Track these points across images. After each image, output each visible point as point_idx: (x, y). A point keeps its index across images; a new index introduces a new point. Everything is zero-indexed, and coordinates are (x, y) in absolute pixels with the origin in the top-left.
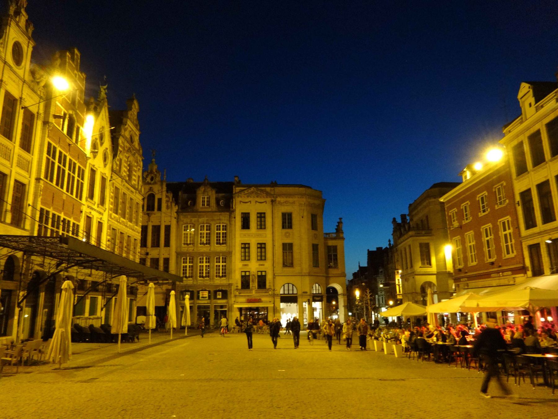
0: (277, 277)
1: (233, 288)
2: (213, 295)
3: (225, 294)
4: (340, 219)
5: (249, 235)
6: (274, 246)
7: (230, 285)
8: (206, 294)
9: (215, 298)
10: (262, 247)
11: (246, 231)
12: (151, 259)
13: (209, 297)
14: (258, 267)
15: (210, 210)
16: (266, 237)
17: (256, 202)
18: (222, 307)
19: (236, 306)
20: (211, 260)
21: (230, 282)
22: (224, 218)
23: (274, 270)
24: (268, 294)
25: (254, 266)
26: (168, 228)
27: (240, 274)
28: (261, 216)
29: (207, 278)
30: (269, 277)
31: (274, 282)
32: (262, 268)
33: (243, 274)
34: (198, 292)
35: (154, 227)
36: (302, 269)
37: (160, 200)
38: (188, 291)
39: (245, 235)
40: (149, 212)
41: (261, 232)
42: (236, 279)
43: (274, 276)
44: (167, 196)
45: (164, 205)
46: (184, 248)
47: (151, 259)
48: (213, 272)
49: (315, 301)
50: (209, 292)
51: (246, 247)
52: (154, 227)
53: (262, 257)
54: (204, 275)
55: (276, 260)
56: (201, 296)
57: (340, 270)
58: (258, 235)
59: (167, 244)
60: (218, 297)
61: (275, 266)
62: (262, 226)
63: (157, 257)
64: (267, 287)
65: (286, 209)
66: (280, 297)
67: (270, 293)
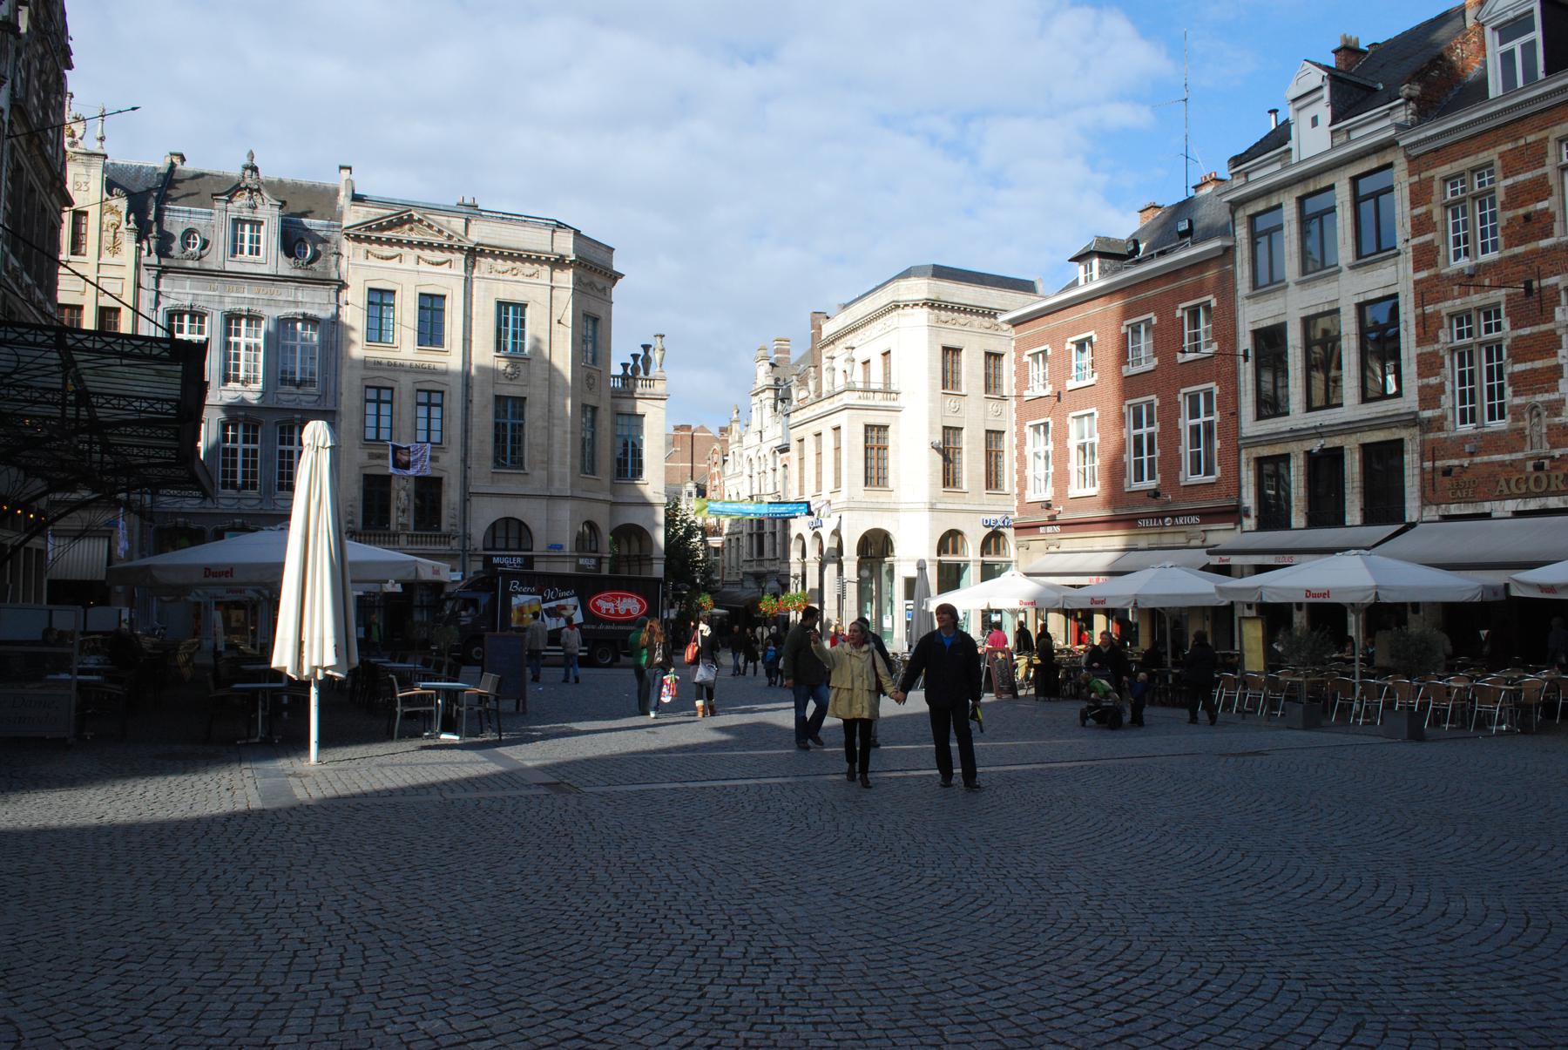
0: (474, 499)
23: (465, 477)
30: (451, 496)
31: (465, 512)
43: (467, 496)
64: (445, 527)
66: (481, 558)
67: (455, 544)
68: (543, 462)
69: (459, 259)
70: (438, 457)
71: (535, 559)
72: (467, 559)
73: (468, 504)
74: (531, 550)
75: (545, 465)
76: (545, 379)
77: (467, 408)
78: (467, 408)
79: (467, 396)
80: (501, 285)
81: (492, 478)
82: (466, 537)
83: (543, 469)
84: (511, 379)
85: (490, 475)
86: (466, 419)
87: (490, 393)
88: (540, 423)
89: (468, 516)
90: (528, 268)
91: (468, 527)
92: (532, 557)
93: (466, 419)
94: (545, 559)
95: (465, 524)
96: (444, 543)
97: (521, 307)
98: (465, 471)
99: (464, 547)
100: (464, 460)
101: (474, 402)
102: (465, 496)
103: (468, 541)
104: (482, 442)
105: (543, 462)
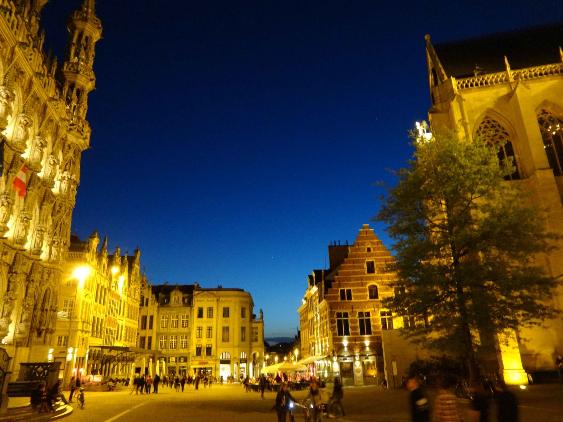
2: (178, 360)
3: (186, 360)
5: (202, 322)
7: (189, 354)
8: (174, 359)
9: (180, 361)
10: (210, 329)
11: (200, 319)
13: (176, 361)
15: (179, 306)
18: (183, 367)
19: (192, 367)
20: (178, 338)
21: (189, 351)
22: (187, 310)
25: (204, 342)
26: (152, 317)
28: (210, 310)
29: (175, 349)
30: (213, 349)
32: (209, 343)
33: (198, 346)
34: (169, 358)
36: (234, 343)
38: (163, 357)
41: (210, 320)
42: (193, 350)
45: (150, 303)
46: (162, 330)
48: (179, 345)
49: (241, 363)
50: (176, 358)
51: (200, 329)
53: (209, 336)
54: (173, 347)
55: (218, 337)
56: (171, 360)
58: (208, 322)
59: (151, 327)
60: (181, 361)
62: (210, 316)
64: (212, 354)
65: (226, 305)
97: (228, 309)
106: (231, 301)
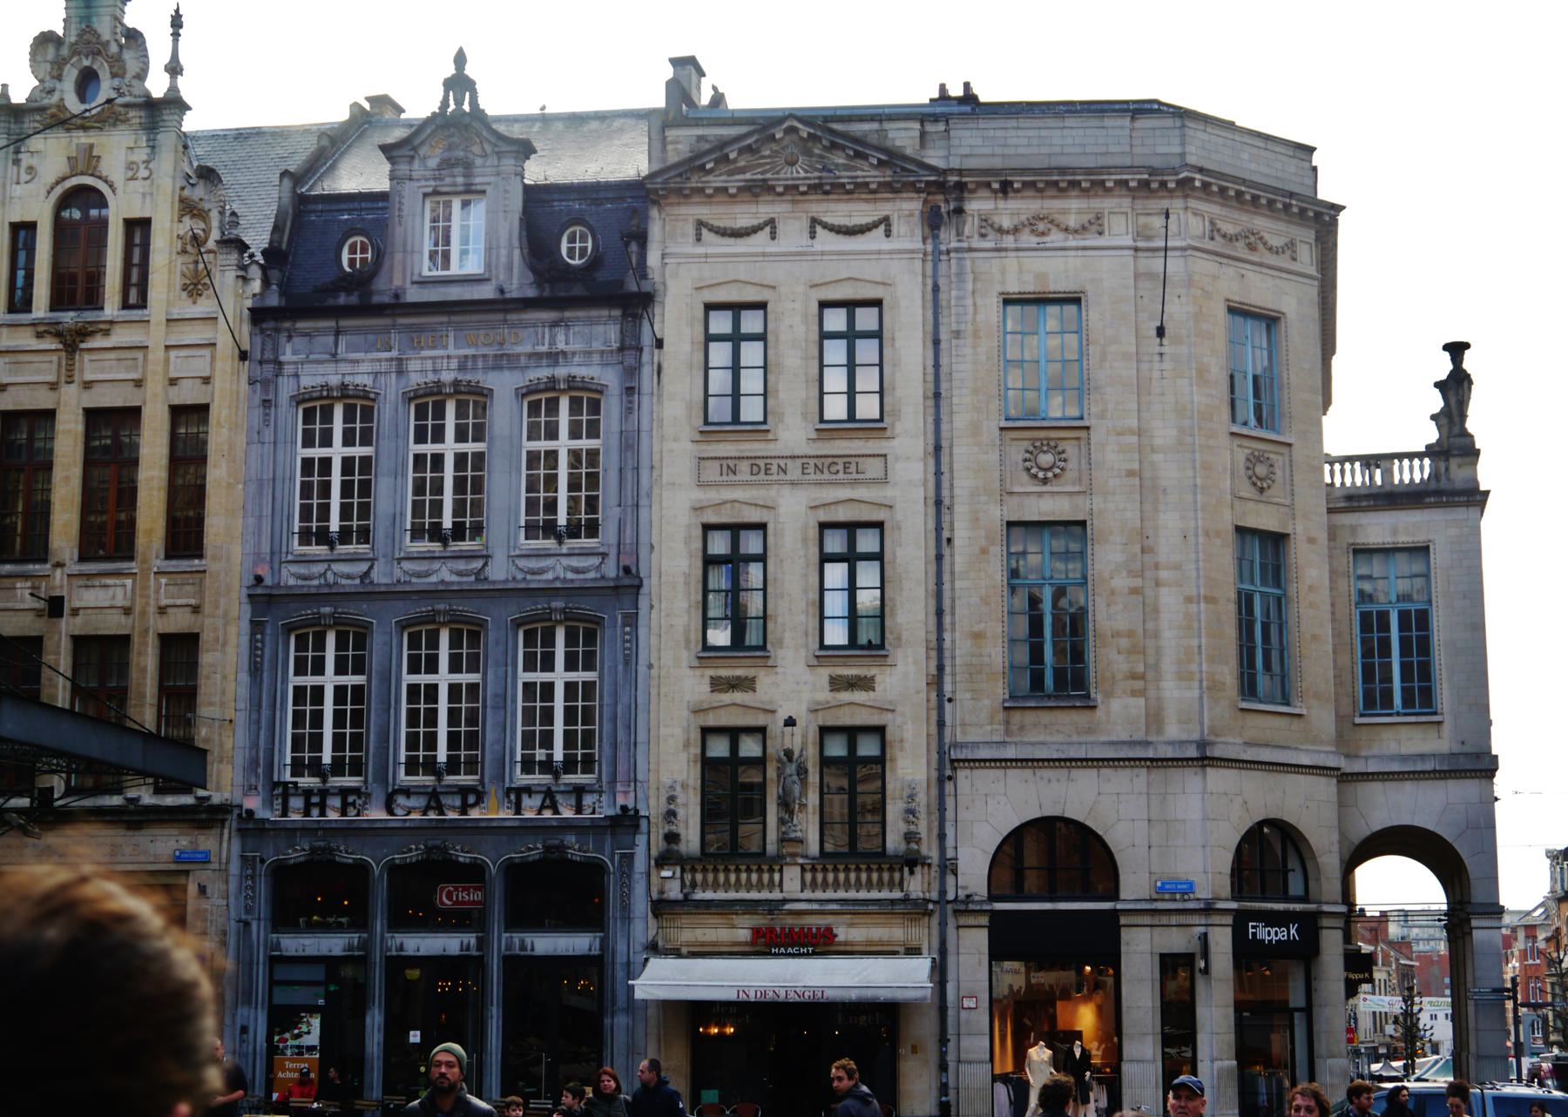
1: (644, 848)
4: (1456, 350)
5: (761, 466)
6: (942, 542)
7: (627, 822)
12: (79, 642)
14: (824, 695)
16: (884, 481)
17: (814, 222)
23: (941, 724)
24: (897, 894)
27: (696, 750)
31: (942, 809)
32: (855, 709)
33: (719, 748)
35: (95, 417)
36: (1155, 718)
37: (138, 228)
39: (729, 466)
40: (68, 318)
44: (189, 208)
47: (79, 642)
52: (95, 417)
55: (960, 646)
57: (1447, 728)
61: (948, 688)
63: (113, 624)
66: (984, 920)
67: (916, 885)
68: (1134, 676)
69: (906, 210)
70: (872, 679)
71: (1123, 920)
72: (951, 922)
73: (949, 787)
74: (1115, 897)
75: (1139, 684)
76: (1131, 473)
77: (939, 557)
78: (939, 557)
79: (939, 529)
80: (1011, 261)
81: (1007, 722)
82: (948, 867)
83: (1134, 693)
84: (1045, 481)
85: (1001, 716)
86: (939, 583)
87: (996, 514)
88: (1121, 582)
89: (950, 814)
90: (1073, 209)
91: (950, 842)
92: (1115, 913)
93: (939, 583)
94: (1147, 920)
95: (942, 836)
96: (891, 885)
98: (941, 708)
99: (943, 892)
100: (937, 681)
101: (957, 542)
102: (940, 769)
103: (950, 879)
104: (977, 636)
105: (1134, 676)
106: (1095, 225)
